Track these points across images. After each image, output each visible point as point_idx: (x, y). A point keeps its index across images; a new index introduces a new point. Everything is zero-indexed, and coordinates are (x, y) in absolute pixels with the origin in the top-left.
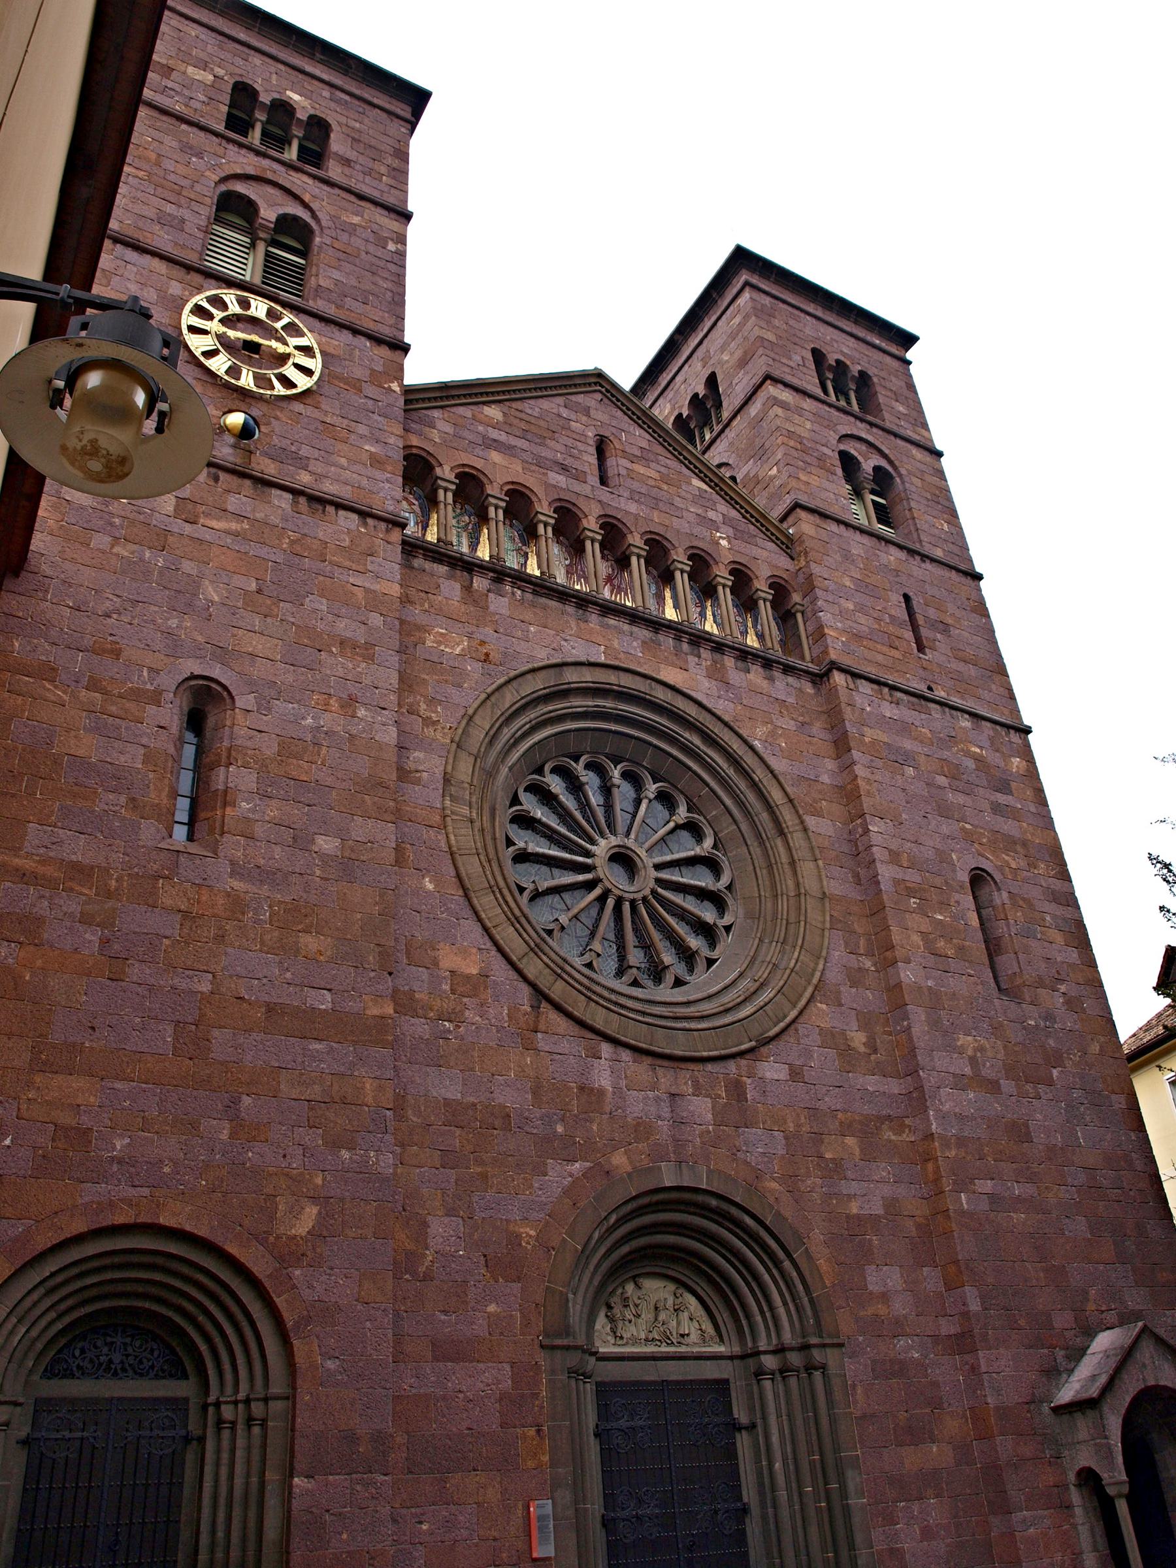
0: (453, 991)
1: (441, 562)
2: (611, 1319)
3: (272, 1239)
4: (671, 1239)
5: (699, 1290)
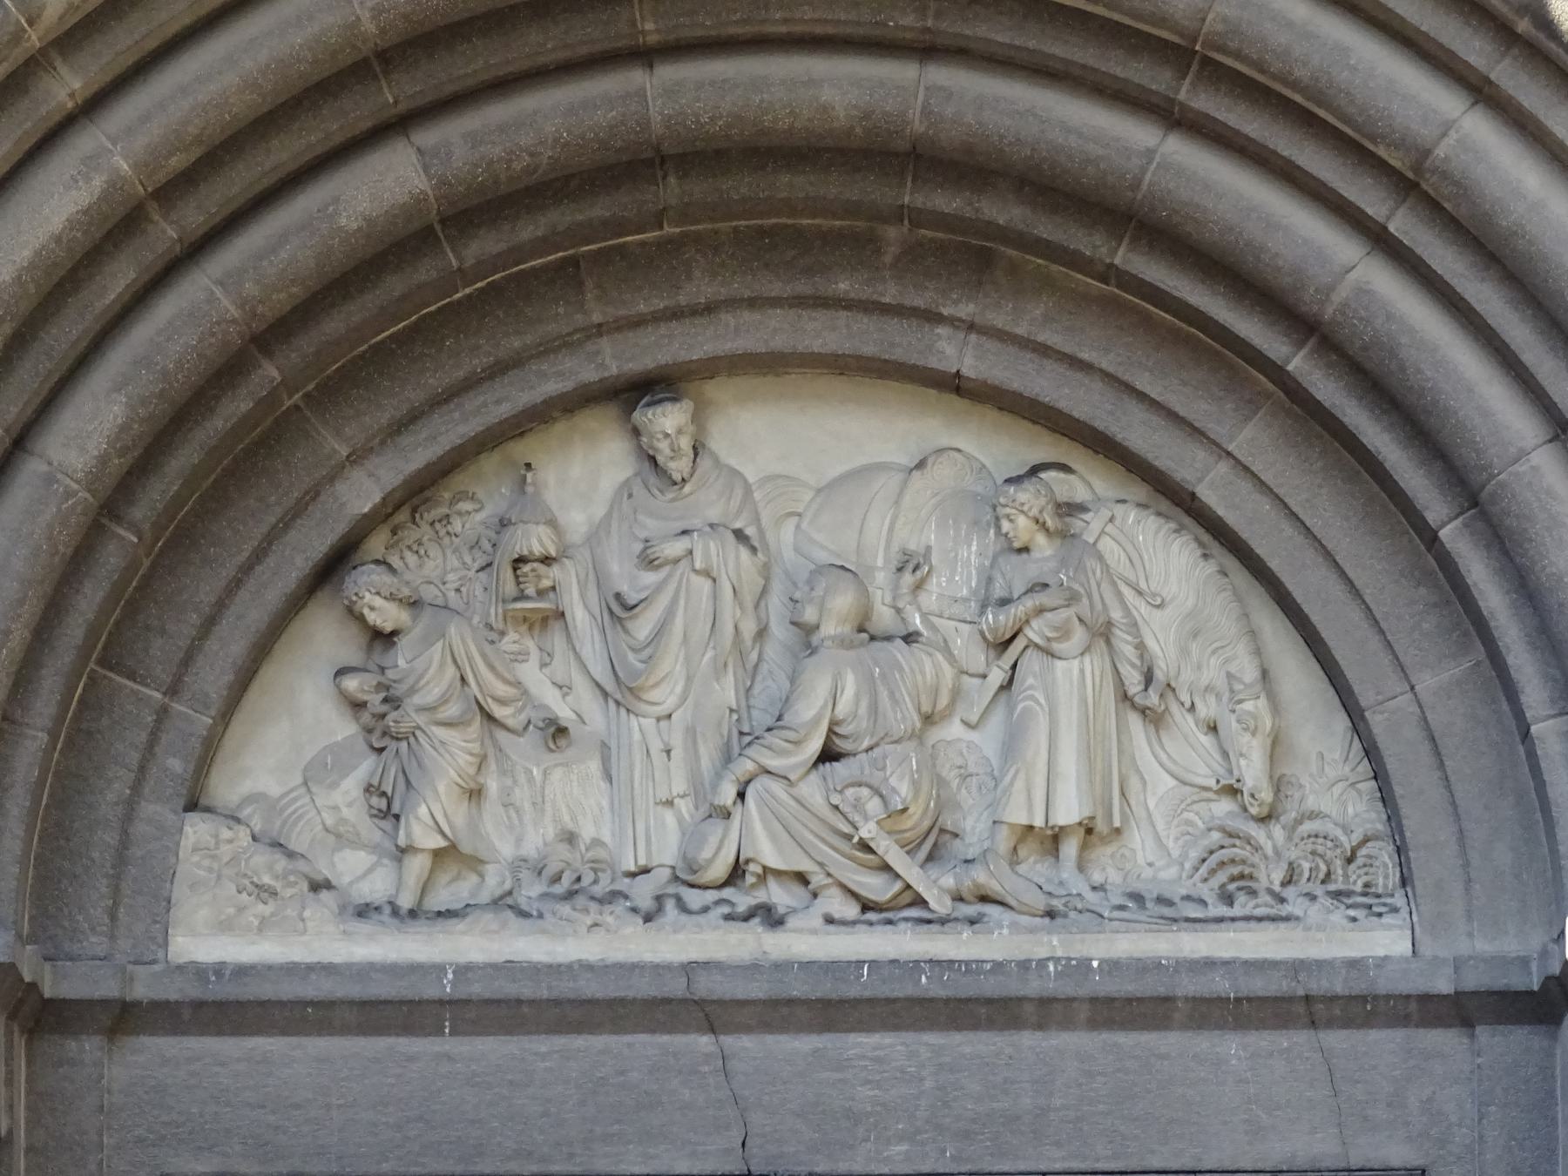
2: (382, 722)
5: (1215, 489)
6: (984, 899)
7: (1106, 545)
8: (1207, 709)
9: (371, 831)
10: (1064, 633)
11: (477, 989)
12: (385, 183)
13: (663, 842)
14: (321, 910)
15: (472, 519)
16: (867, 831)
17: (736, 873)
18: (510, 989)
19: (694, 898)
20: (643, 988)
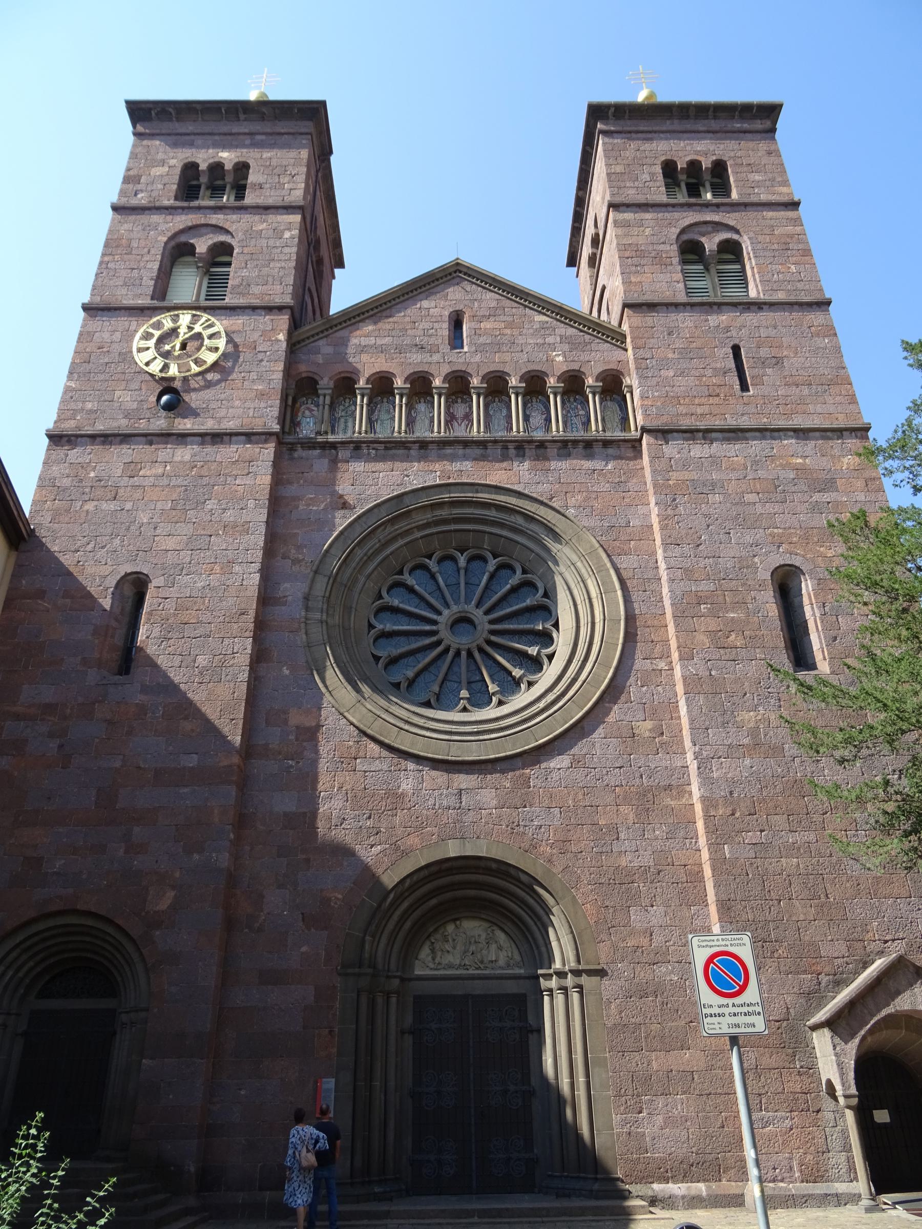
0: (297, 740)
1: (314, 448)
2: (433, 951)
3: (143, 914)
4: (472, 893)
5: (506, 929)
12: (434, 902)
13: (458, 962)
15: (441, 932)
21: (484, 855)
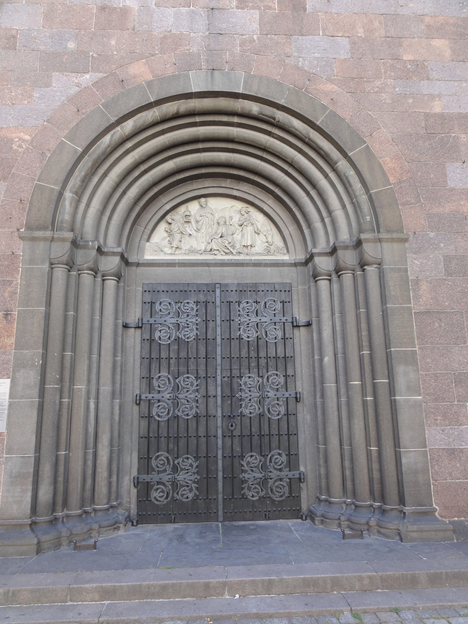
2: (170, 233)
6: (240, 253)
7: (253, 215)
8: (265, 233)
9: (169, 246)
10: (248, 224)
11: (181, 262)
14: (161, 253)
16: (226, 245)
17: (211, 250)
18: (184, 262)
19: (206, 253)
20: (200, 262)
21: (240, 92)
